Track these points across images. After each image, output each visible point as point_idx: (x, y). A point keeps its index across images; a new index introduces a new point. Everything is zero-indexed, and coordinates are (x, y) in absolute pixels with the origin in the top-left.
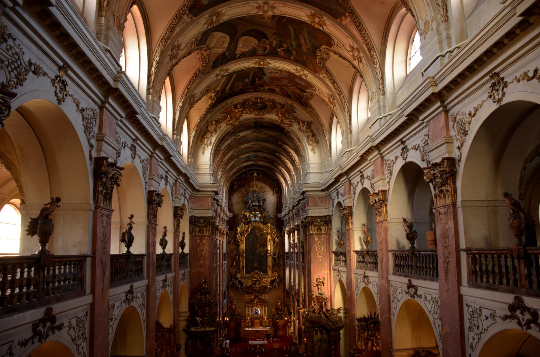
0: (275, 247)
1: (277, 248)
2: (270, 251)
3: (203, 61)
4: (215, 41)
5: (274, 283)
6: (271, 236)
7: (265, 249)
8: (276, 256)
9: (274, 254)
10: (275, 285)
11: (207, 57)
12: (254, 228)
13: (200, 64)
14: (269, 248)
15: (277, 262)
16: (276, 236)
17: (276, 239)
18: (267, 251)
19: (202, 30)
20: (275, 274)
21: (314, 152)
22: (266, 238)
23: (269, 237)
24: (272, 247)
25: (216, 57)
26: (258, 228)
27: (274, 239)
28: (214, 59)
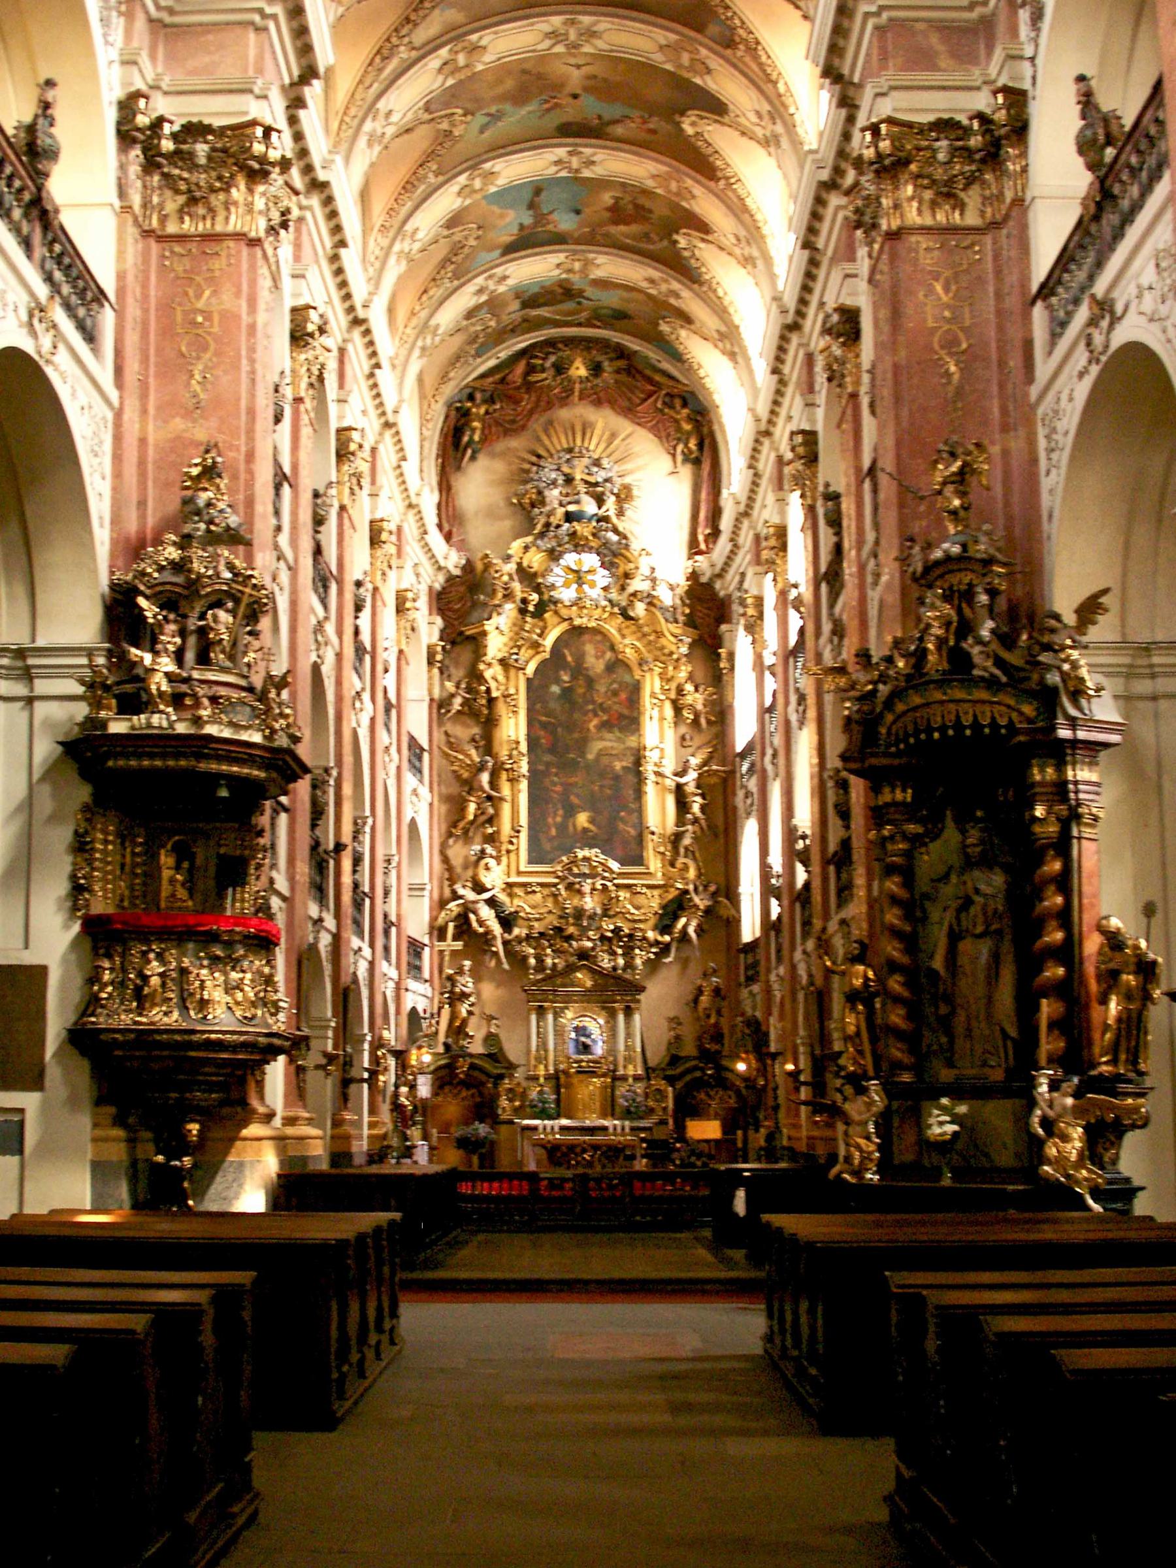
0: (683, 738)
5: (676, 918)
6: (662, 676)
7: (632, 741)
8: (692, 776)
10: (685, 927)
12: (576, 632)
16: (691, 678)
17: (689, 687)
20: (686, 868)
22: (636, 688)
23: (652, 684)
26: (596, 631)
27: (680, 691)
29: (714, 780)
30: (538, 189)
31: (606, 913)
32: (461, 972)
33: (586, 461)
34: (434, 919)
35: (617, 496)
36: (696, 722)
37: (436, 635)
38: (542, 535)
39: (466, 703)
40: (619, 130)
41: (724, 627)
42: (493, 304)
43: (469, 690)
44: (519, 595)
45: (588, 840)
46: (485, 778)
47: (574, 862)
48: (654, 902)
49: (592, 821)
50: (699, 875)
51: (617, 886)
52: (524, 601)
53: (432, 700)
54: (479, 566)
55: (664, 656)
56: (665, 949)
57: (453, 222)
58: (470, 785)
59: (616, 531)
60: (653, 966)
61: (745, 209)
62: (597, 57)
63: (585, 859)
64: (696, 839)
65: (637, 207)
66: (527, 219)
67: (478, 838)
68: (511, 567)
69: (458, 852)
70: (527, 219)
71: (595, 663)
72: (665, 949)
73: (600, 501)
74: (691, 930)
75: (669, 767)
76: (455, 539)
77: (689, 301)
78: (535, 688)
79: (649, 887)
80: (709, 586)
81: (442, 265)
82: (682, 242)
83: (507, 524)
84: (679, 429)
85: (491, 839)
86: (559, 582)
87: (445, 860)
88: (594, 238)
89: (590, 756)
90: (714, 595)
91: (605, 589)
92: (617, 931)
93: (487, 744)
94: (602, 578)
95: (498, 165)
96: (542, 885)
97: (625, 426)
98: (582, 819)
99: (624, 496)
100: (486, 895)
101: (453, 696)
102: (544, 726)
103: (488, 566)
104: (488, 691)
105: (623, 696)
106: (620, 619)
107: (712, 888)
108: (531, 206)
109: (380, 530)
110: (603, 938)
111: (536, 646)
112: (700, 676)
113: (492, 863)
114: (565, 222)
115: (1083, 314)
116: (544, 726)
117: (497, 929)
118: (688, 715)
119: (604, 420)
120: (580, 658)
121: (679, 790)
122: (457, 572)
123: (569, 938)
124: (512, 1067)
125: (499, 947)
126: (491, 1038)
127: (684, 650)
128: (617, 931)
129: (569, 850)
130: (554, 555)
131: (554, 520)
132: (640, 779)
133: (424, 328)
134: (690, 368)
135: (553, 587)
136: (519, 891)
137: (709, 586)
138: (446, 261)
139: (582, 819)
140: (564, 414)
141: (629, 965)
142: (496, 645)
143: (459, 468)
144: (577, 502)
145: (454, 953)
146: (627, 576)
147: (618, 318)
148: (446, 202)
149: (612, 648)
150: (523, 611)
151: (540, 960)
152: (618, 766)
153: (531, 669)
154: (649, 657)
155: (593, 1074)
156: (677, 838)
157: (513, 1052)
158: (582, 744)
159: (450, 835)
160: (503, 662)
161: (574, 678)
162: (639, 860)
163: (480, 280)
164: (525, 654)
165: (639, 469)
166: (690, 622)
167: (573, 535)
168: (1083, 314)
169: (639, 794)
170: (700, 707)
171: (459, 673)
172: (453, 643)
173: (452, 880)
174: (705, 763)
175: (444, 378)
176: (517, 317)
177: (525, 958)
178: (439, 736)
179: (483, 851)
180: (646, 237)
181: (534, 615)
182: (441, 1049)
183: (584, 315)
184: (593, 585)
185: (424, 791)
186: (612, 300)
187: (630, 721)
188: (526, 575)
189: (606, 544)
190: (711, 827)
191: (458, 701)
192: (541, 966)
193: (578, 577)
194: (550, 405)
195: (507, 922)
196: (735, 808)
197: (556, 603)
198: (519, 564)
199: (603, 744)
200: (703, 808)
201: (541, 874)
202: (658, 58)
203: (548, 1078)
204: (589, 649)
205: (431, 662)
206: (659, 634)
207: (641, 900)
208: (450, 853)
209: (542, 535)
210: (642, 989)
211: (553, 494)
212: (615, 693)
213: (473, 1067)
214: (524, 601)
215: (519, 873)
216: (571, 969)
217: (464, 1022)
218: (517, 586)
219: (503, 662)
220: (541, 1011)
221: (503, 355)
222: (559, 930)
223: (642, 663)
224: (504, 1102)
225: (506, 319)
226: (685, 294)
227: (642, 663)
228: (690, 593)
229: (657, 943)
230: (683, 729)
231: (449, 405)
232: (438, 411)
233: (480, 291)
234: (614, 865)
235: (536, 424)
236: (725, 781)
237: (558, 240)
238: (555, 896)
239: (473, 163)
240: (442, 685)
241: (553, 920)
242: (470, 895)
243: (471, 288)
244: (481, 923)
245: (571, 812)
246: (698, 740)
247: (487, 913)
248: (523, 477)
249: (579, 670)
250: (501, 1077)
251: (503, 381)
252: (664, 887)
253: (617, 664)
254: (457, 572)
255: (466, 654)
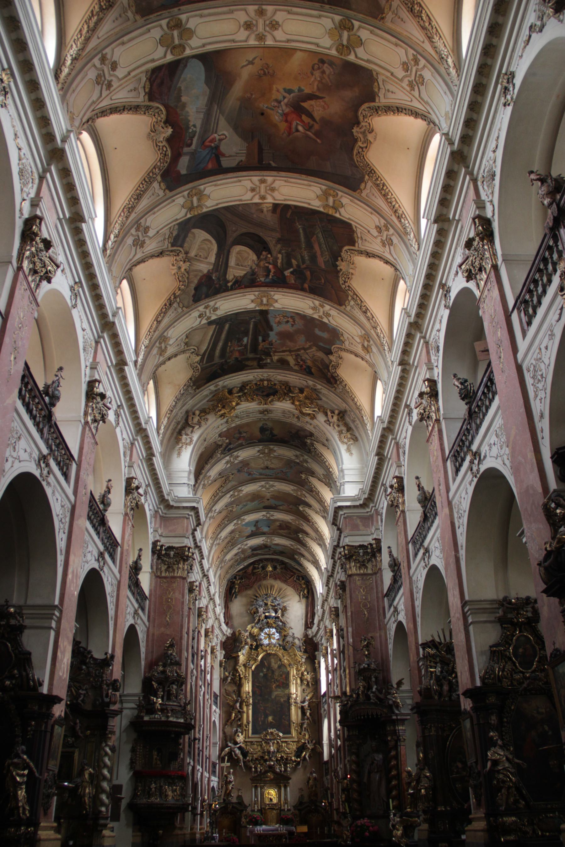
0: (304, 690)
1: (308, 692)
2: (294, 696)
3: (180, 281)
4: (197, 247)
5: (302, 752)
6: (297, 670)
7: (287, 692)
8: (306, 704)
9: (303, 702)
10: (305, 755)
11: (187, 275)
13: (176, 284)
14: (293, 689)
15: (308, 714)
16: (306, 670)
17: (305, 673)
18: (289, 696)
19: (178, 217)
20: (305, 735)
21: (351, 454)
22: (288, 673)
24: (299, 689)
25: (199, 277)
26: (275, 655)
27: (302, 674)
28: (196, 281)
29: (314, 704)
30: (257, 522)
31: (278, 751)
32: (229, 773)
33: (272, 598)
34: (220, 754)
35: (282, 610)
36: (308, 685)
37: (222, 657)
38: (258, 623)
39: (232, 679)
40: (281, 508)
41: (316, 653)
42: (243, 551)
43: (233, 675)
44: (250, 643)
45: (272, 726)
46: (238, 705)
47: (268, 733)
48: (294, 747)
49: (273, 719)
50: (309, 737)
51: (282, 742)
52: (252, 645)
53: (221, 679)
54: (237, 634)
55: (297, 663)
56: (298, 763)
57: (232, 532)
58: (233, 707)
59: (281, 621)
60: (294, 769)
61: (318, 531)
62: (275, 491)
63: (272, 733)
64: (308, 724)
65: (287, 526)
66: (254, 529)
67: (235, 725)
68: (247, 634)
69: (228, 729)
70: (254, 529)
71: (275, 665)
72: (298, 763)
73: (276, 612)
74: (307, 756)
75: (299, 699)
76: (229, 624)
77: (303, 551)
78: (255, 674)
79: (293, 742)
80: (312, 639)
81: (228, 543)
82: (301, 536)
83: (246, 619)
84: (301, 587)
85: (240, 726)
86: (263, 638)
87: (224, 733)
88: (274, 533)
89: (273, 697)
90: (314, 642)
91: (278, 640)
92: (282, 757)
93: (239, 692)
94: (277, 636)
95: (245, 517)
96: (257, 742)
97: (284, 586)
98: (270, 718)
99: (284, 610)
100: (238, 746)
101: (227, 677)
102: (258, 687)
103: (240, 634)
104: (240, 675)
105: (284, 676)
106: (282, 651)
107: (314, 742)
108: (255, 526)
109: (208, 632)
110: (277, 760)
111: (255, 660)
112: (309, 669)
113: (240, 734)
114: (266, 529)
115: (422, 551)
116: (258, 687)
117: (241, 757)
118: (305, 682)
119: (278, 584)
120: (270, 664)
121: (302, 708)
122: (230, 635)
123: (266, 761)
124: (246, 807)
125: (242, 764)
126: (239, 797)
127: (304, 660)
128: (282, 757)
129: (266, 730)
130: (261, 629)
131: (261, 619)
132: (289, 705)
133: (222, 561)
134: (304, 568)
135: (261, 640)
136: (249, 744)
137: (312, 639)
138: (229, 542)
139: (270, 718)
140: (265, 582)
141: (286, 770)
142: (242, 657)
143: (231, 601)
144: (269, 612)
145: (227, 767)
146: (285, 636)
147: (281, 553)
148: (230, 527)
149: (280, 660)
150: (251, 648)
151: (256, 768)
152: (282, 700)
153: (253, 667)
154: (292, 663)
155: (273, 809)
156: (302, 724)
157: (246, 801)
158: (270, 693)
159: (226, 724)
160: (244, 665)
161: (268, 670)
162: (289, 732)
163: (239, 546)
164: (252, 662)
165: (289, 600)
166: (305, 651)
167: (267, 623)
168: (422, 551)
169: (289, 710)
170: (309, 679)
171: (230, 669)
172: (228, 659)
173: (226, 741)
174: (311, 698)
175: (227, 572)
176: (250, 553)
177: (251, 768)
178: (222, 690)
179: (237, 730)
180: (290, 533)
181: (254, 649)
182: (222, 801)
183: (271, 552)
184: (274, 638)
185: (218, 710)
186: (279, 548)
187: (286, 685)
188: (252, 636)
189: (278, 625)
190: (314, 720)
191: (229, 678)
192: (256, 771)
193: (269, 636)
194: (260, 580)
195: (245, 753)
196: (321, 714)
197: (262, 645)
198: (250, 633)
199: (277, 693)
200: (310, 714)
201: (256, 738)
202: (292, 492)
203: (258, 811)
204: (273, 660)
205: (221, 666)
206: (295, 655)
207: (290, 746)
208: (226, 730)
209: (258, 623)
210: (290, 779)
211: (261, 610)
212: (281, 676)
213: (233, 807)
214: (252, 645)
215: (249, 737)
216: (266, 772)
217: (230, 791)
218: (249, 640)
219: (244, 665)
220: (256, 787)
221: (245, 564)
222: (262, 757)
223: (290, 665)
224: (243, 820)
225: (247, 554)
226: (302, 549)
227: (290, 665)
228: (305, 642)
229: (295, 761)
230: (304, 687)
231: (228, 581)
232: (225, 582)
233: (239, 549)
234: (281, 734)
235: (256, 586)
236: (318, 705)
237: (264, 534)
238: (261, 746)
239: (238, 517)
240: (224, 674)
241: (260, 754)
242: (233, 746)
243: (236, 548)
244: (236, 755)
245: (266, 716)
246: (309, 690)
247: (238, 751)
248: (251, 604)
249: (269, 668)
250: (243, 811)
251: (245, 572)
252: (298, 742)
253: (282, 666)
254: (230, 635)
255: (232, 663)
